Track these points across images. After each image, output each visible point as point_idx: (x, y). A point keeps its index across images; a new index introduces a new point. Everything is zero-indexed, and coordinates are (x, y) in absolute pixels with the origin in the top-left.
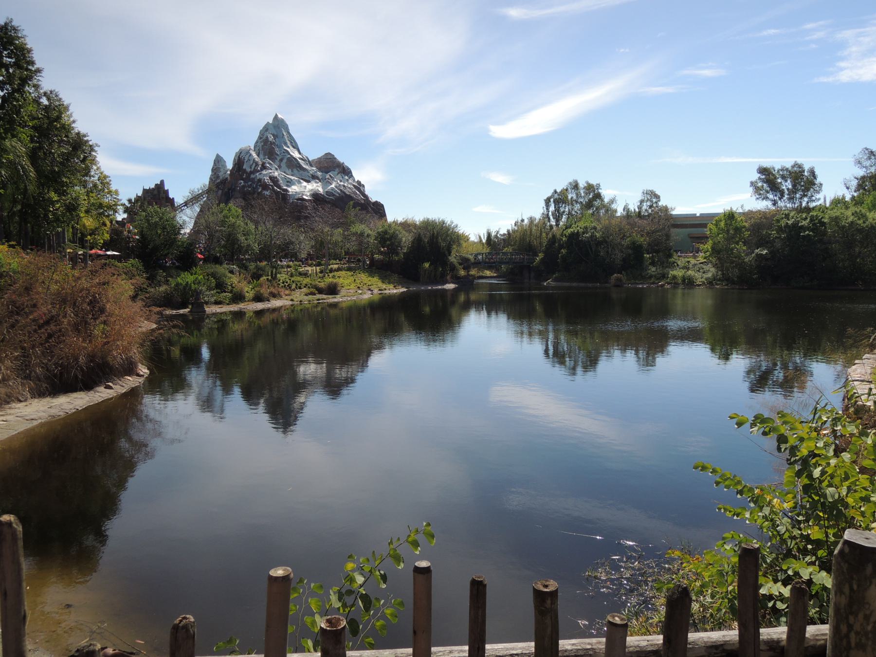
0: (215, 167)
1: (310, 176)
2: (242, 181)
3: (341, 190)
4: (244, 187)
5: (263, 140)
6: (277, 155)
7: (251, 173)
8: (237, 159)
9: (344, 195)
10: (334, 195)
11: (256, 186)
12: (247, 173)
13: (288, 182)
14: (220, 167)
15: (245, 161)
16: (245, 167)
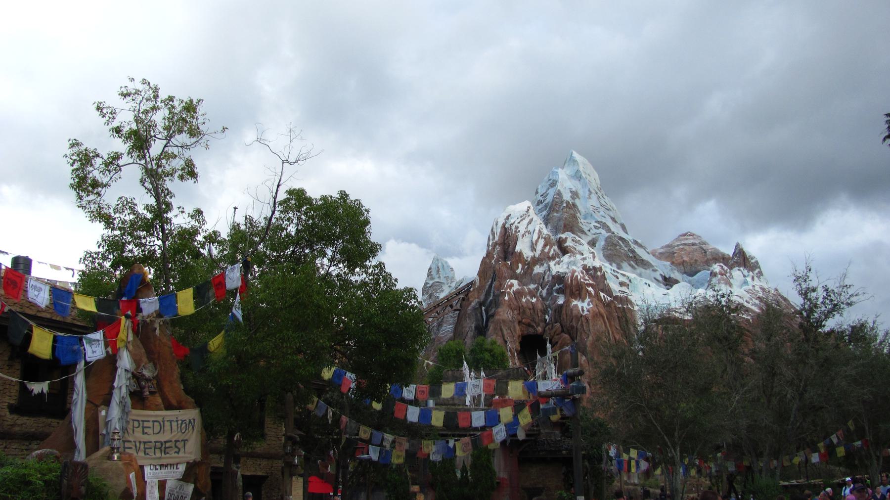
0: (431, 282)
1: (660, 279)
2: (515, 282)
4: (518, 294)
5: (546, 206)
6: (583, 232)
7: (536, 261)
8: (498, 230)
11: (549, 293)
12: (525, 263)
14: (442, 280)
15: (520, 234)
16: (523, 247)
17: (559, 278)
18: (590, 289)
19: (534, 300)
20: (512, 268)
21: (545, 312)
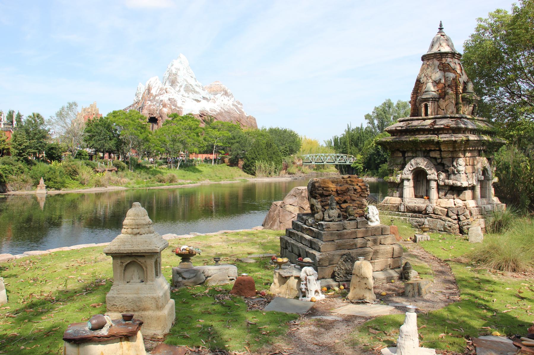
0: (138, 92)
1: (202, 97)
2: (149, 102)
3: (221, 108)
4: (150, 106)
6: (178, 83)
7: (156, 96)
9: (223, 111)
10: (215, 111)
11: (159, 105)
13: (183, 102)
16: (153, 92)
17: (162, 101)
18: (168, 105)
19: (154, 107)
20: (149, 98)
21: (157, 110)
